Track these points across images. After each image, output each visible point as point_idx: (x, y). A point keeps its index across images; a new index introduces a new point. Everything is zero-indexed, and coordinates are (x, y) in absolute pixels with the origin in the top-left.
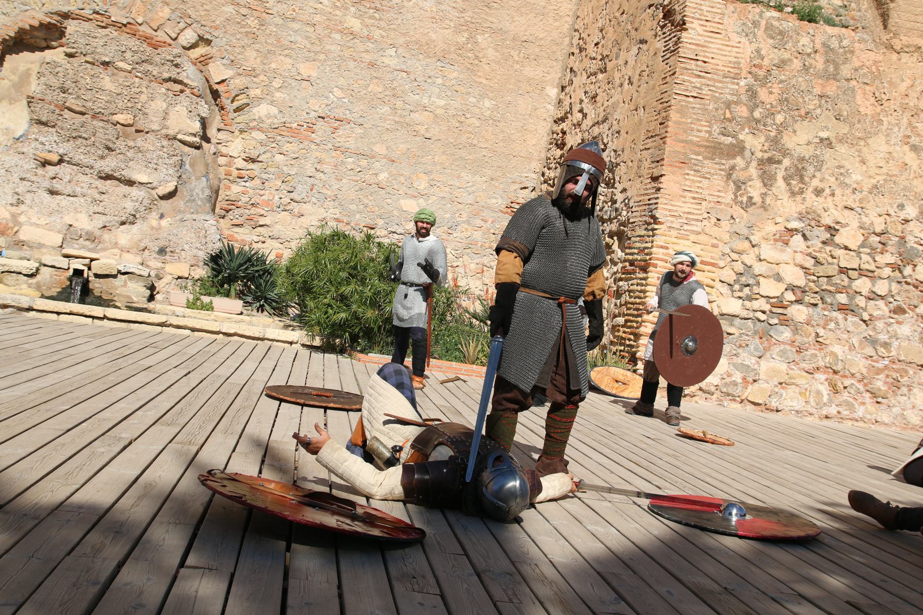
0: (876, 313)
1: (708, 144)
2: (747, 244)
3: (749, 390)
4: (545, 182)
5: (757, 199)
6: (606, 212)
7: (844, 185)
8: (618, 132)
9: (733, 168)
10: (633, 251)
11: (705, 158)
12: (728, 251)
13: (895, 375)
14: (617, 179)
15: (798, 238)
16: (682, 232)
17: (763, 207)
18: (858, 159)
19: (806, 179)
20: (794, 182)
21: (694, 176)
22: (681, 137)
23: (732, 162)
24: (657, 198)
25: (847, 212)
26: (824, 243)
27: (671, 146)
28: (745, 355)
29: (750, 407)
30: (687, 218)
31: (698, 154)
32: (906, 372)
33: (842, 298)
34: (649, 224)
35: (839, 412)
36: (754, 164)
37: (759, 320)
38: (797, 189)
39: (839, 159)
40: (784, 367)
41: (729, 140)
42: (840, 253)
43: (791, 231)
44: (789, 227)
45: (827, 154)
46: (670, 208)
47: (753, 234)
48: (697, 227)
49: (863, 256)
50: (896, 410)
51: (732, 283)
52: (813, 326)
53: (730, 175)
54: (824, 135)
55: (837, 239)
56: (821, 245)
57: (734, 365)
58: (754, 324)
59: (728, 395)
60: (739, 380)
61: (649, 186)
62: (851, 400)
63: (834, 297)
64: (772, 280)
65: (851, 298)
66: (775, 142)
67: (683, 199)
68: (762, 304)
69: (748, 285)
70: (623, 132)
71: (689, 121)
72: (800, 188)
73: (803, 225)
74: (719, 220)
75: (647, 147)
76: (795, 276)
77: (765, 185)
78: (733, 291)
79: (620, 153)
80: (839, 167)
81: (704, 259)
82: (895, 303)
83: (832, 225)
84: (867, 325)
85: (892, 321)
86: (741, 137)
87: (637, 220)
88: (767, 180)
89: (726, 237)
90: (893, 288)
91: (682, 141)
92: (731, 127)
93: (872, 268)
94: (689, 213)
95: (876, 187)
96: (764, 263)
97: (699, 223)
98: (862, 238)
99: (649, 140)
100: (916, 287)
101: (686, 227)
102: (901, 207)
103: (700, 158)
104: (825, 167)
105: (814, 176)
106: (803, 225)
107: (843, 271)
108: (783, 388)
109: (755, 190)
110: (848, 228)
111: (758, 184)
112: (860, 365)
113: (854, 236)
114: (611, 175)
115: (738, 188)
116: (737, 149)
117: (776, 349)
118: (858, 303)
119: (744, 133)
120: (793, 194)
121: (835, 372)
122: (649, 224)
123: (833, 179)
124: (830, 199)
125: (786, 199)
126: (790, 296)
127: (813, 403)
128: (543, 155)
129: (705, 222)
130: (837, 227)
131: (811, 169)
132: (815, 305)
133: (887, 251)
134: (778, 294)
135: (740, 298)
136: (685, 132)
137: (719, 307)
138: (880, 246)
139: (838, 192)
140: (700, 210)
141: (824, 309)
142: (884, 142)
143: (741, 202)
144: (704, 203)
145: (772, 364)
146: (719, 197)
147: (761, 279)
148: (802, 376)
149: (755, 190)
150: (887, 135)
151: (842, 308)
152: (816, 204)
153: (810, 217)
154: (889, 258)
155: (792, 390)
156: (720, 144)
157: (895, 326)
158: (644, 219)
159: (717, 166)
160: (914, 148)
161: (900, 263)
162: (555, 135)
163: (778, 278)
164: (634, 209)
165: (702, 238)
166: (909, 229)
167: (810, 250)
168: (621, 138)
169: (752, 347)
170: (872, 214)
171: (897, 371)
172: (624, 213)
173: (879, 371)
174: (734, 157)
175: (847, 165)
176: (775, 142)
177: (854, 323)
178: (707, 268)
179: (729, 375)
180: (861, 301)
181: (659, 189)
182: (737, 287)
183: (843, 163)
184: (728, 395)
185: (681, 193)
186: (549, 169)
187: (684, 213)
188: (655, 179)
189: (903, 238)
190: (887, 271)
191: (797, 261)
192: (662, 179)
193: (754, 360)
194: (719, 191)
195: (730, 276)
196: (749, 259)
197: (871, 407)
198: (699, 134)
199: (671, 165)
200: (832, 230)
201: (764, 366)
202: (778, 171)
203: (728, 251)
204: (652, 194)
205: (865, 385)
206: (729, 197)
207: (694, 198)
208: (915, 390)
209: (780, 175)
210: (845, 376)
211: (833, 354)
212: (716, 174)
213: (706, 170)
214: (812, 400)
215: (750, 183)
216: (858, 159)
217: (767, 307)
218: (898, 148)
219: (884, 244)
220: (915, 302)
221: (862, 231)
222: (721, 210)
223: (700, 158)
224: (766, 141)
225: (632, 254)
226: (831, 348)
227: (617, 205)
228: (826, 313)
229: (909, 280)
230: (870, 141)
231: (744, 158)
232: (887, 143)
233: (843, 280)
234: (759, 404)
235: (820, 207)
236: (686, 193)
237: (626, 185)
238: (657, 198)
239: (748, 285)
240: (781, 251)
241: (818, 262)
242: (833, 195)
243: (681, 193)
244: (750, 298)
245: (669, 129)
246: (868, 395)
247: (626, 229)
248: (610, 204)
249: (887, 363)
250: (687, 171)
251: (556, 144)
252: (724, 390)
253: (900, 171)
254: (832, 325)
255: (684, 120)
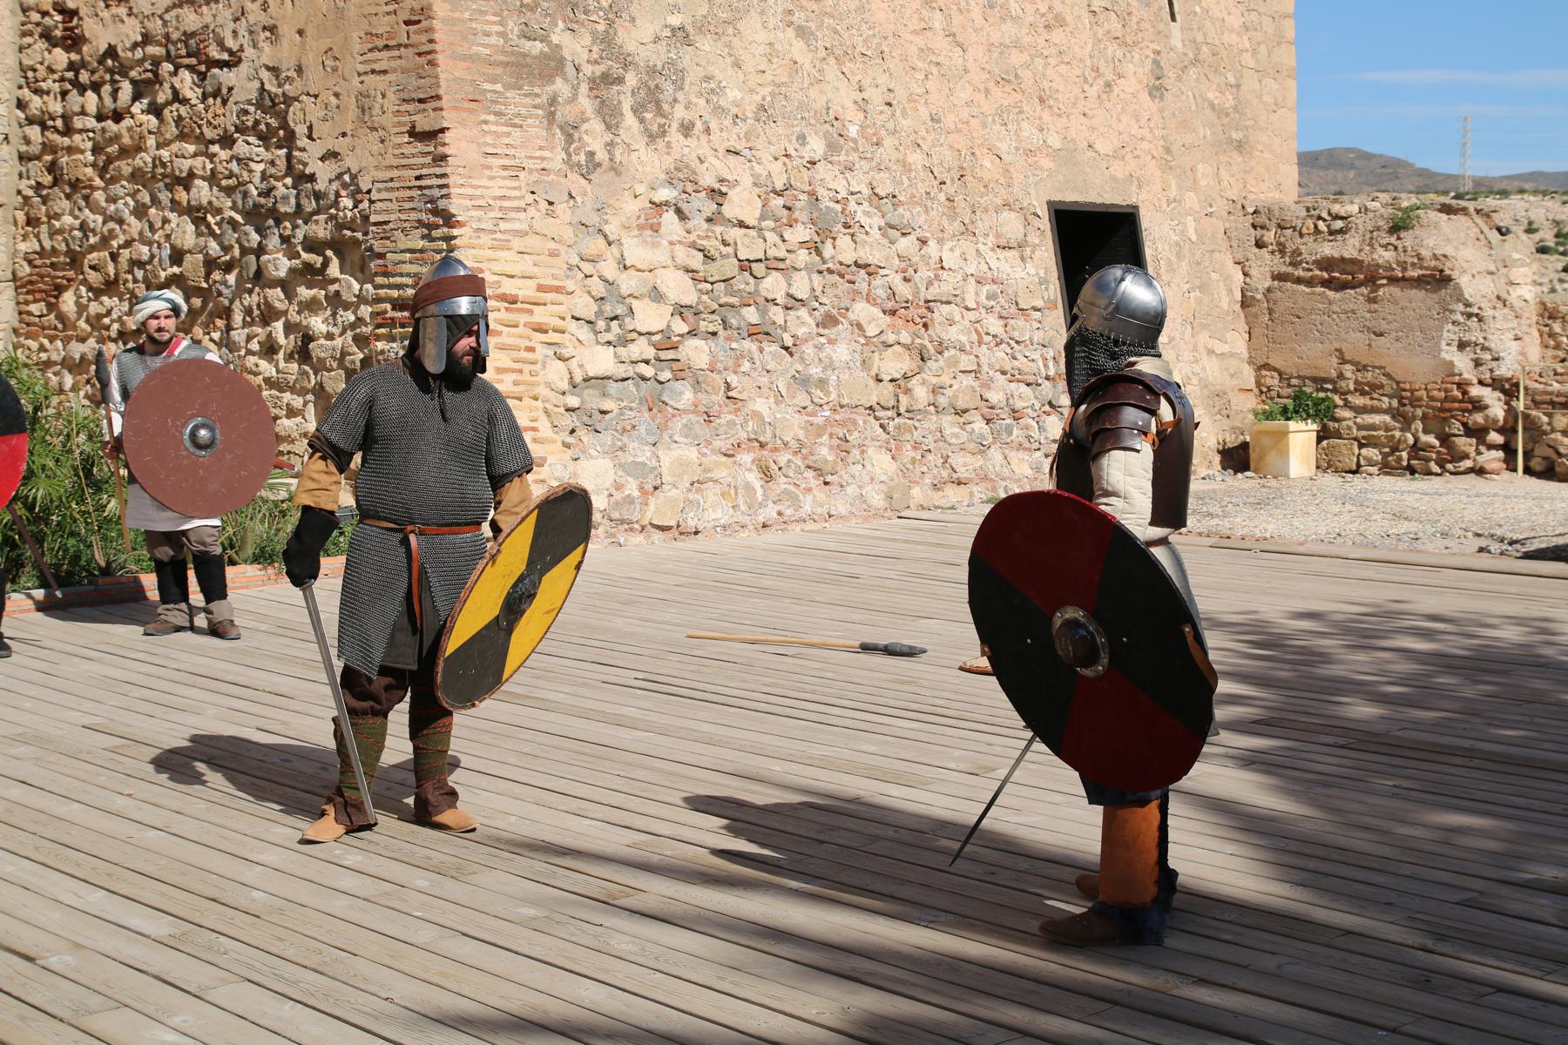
0: (801, 331)
1: (501, 58)
2: (601, 241)
3: (652, 507)
4: (31, 121)
5: (601, 156)
6: (285, 198)
7: (719, 111)
8: (272, 29)
9: (553, 101)
10: (398, 280)
11: (507, 87)
12: (575, 260)
13: (840, 432)
14: (301, 130)
15: (670, 217)
16: (498, 236)
17: (612, 168)
18: (729, 60)
19: (666, 107)
20: (648, 116)
21: (497, 123)
22: (459, 50)
23: (550, 89)
24: (444, 176)
25: (732, 158)
26: (709, 220)
27: (450, 73)
28: (636, 444)
29: (657, 536)
30: (501, 209)
31: (494, 81)
32: (854, 422)
33: (751, 315)
34: (431, 227)
35: (780, 514)
36: (584, 88)
37: (644, 379)
38: (655, 128)
39: (703, 63)
40: (692, 454)
41: (537, 47)
42: (735, 233)
43: (658, 206)
44: (656, 200)
45: (687, 57)
46: (471, 191)
47: (606, 222)
48: (519, 223)
49: (768, 235)
50: (851, 490)
51: (593, 318)
52: (720, 372)
53: (552, 114)
54: (675, 20)
55: (729, 211)
56: (705, 225)
57: (622, 466)
58: (637, 385)
59: (622, 522)
60: (636, 493)
61: (408, 150)
62: (791, 488)
63: (739, 313)
64: (647, 300)
65: (763, 313)
66: (607, 41)
67: (488, 172)
68: (641, 348)
69: (615, 318)
70: (287, 31)
71: (467, 15)
72: (660, 126)
73: (675, 193)
74: (551, 203)
75: (377, 67)
76: (679, 288)
77: (608, 127)
78: (596, 333)
79: (292, 74)
80: (708, 79)
81: (543, 282)
82: (822, 309)
83: (716, 186)
84: (791, 355)
85: (823, 340)
86: (555, 39)
87: (393, 217)
88: (610, 116)
89: (568, 234)
90: (816, 284)
91: (464, 58)
92: (536, 20)
93: (782, 254)
94: (503, 198)
95: (762, 108)
96: (632, 272)
97: (522, 215)
98: (759, 204)
99: (377, 55)
100: (842, 276)
101: (503, 226)
102: (802, 139)
103: (498, 87)
104: (687, 82)
105: (675, 100)
106: (675, 193)
107: (745, 266)
108: (697, 490)
109: (594, 137)
110: (738, 189)
111: (595, 125)
112: (794, 427)
113: (749, 202)
114: (274, 122)
115: (569, 138)
116: (553, 64)
117: (678, 424)
118: (774, 318)
119: (558, 30)
120: (652, 138)
121: (762, 445)
122: (431, 227)
123: (702, 102)
124: (704, 138)
125: (643, 149)
126: (680, 327)
127: (743, 507)
128: (11, 60)
129: (532, 212)
130: (724, 189)
131: (669, 88)
132: (714, 334)
133: (796, 221)
134: (662, 326)
135: (609, 343)
136: (465, 38)
137: (581, 366)
138: (785, 212)
139: (713, 126)
140: (519, 188)
141: (728, 339)
142: (759, 26)
143: (579, 165)
144: (522, 175)
145: (677, 452)
146: (543, 159)
147: (635, 304)
148: (722, 464)
149: (594, 137)
150: (762, 13)
151: (757, 333)
152: (686, 151)
153: (682, 176)
154: (801, 233)
155: (712, 493)
156: (525, 56)
157: (828, 349)
158: (414, 216)
159: (528, 101)
160: (802, 32)
161: (817, 239)
162: (36, 17)
163: (656, 295)
164: (375, 196)
165: (532, 242)
166: (818, 177)
167: (693, 237)
168: (285, 43)
169: (642, 428)
170: (766, 156)
171: (842, 424)
172: (347, 202)
173: (820, 431)
174: (549, 78)
175: (719, 76)
176: (607, 41)
177: (774, 355)
178: (550, 296)
179: (619, 487)
180: (777, 314)
181: (444, 157)
182: (601, 324)
183: (712, 70)
184: (622, 522)
185: (483, 161)
186: (38, 92)
187: (495, 198)
188: (431, 135)
189: (812, 194)
190: (803, 256)
191: (679, 261)
192: (447, 137)
193: (648, 449)
194: (541, 148)
195: (587, 308)
196: (609, 269)
197: (820, 494)
198: (487, 40)
199: (455, 108)
200: (717, 195)
201: (667, 458)
202: (622, 98)
203: (575, 260)
204: (423, 166)
205: (805, 458)
206: (557, 159)
207: (505, 168)
208: (870, 451)
209: (627, 104)
210: (776, 449)
211: (757, 415)
212: (531, 116)
213: (511, 110)
214: (741, 502)
215: (585, 126)
216: (729, 60)
217: (650, 353)
218: (781, 35)
219: (789, 209)
220: (847, 303)
221: (757, 190)
222: (551, 184)
223: (498, 87)
224: (594, 42)
225: (399, 287)
226: (752, 406)
227: (321, 186)
228: (734, 345)
229: (830, 265)
230: (741, 25)
231: (566, 80)
232: (764, 25)
233: (743, 283)
234: (668, 528)
235: (694, 156)
236: (490, 160)
237: (340, 145)
238: (444, 176)
239: (615, 318)
240: (656, 245)
241: (708, 258)
242: (707, 130)
243: (483, 161)
244: (624, 342)
245: (436, 36)
246: (810, 474)
247: (359, 235)
248: (289, 181)
249: (827, 413)
250: (484, 117)
251: (46, 35)
252: (616, 515)
253: (790, 75)
254: (746, 366)
255: (457, 15)
